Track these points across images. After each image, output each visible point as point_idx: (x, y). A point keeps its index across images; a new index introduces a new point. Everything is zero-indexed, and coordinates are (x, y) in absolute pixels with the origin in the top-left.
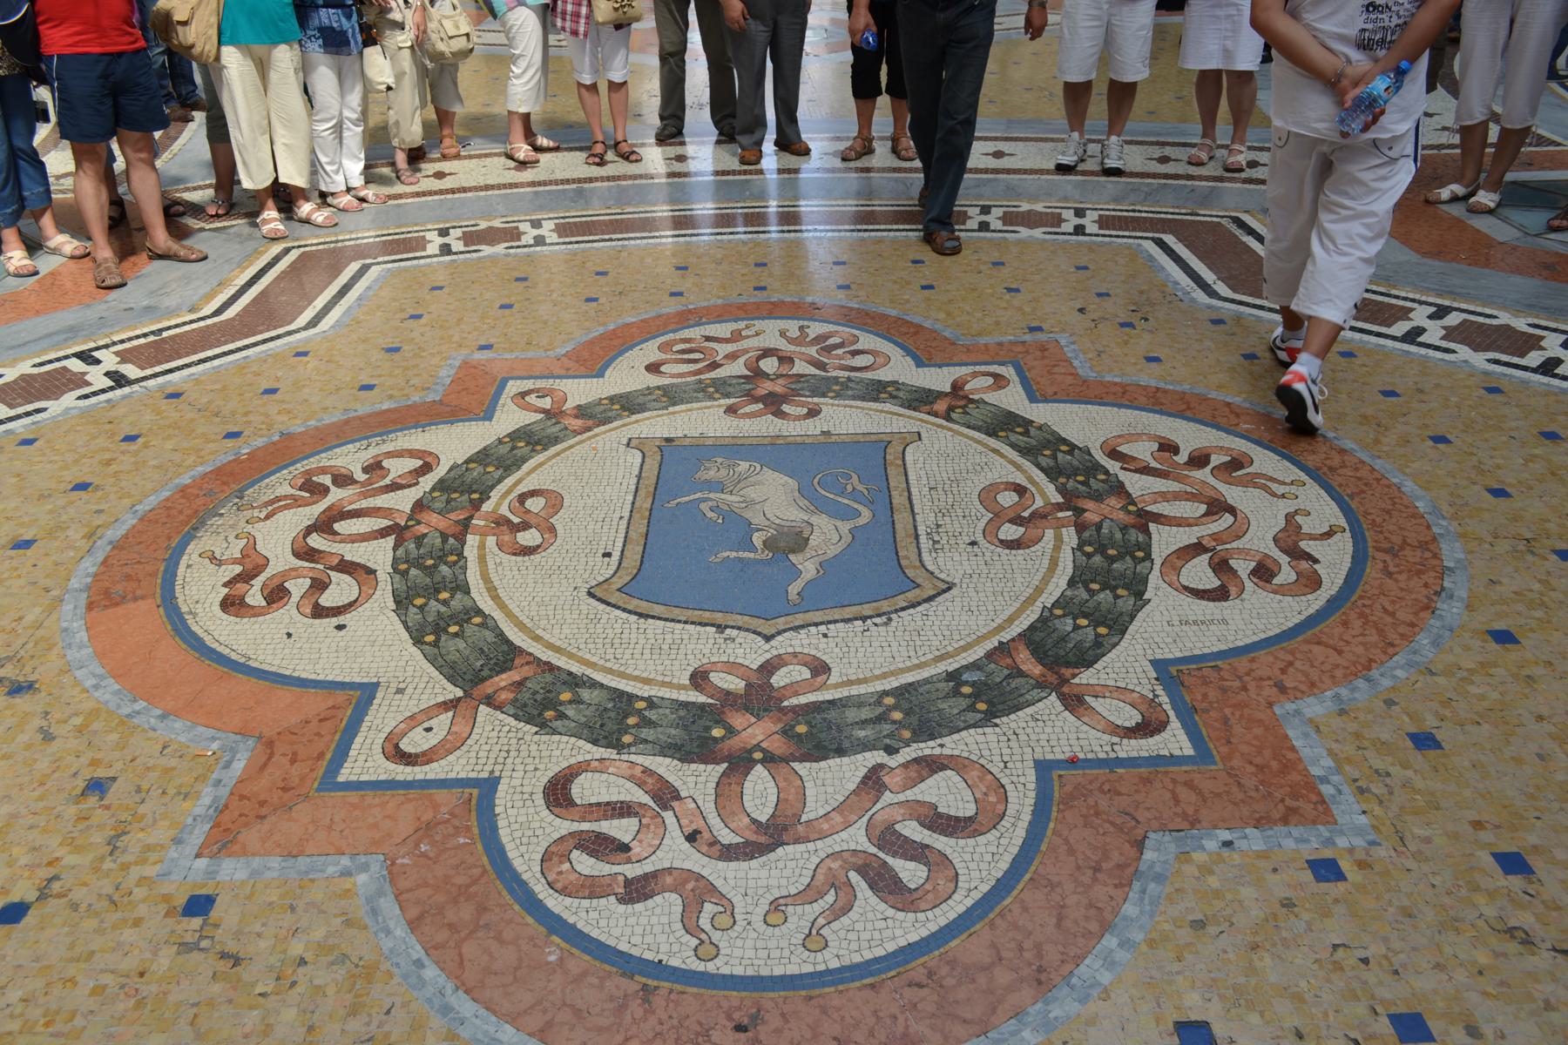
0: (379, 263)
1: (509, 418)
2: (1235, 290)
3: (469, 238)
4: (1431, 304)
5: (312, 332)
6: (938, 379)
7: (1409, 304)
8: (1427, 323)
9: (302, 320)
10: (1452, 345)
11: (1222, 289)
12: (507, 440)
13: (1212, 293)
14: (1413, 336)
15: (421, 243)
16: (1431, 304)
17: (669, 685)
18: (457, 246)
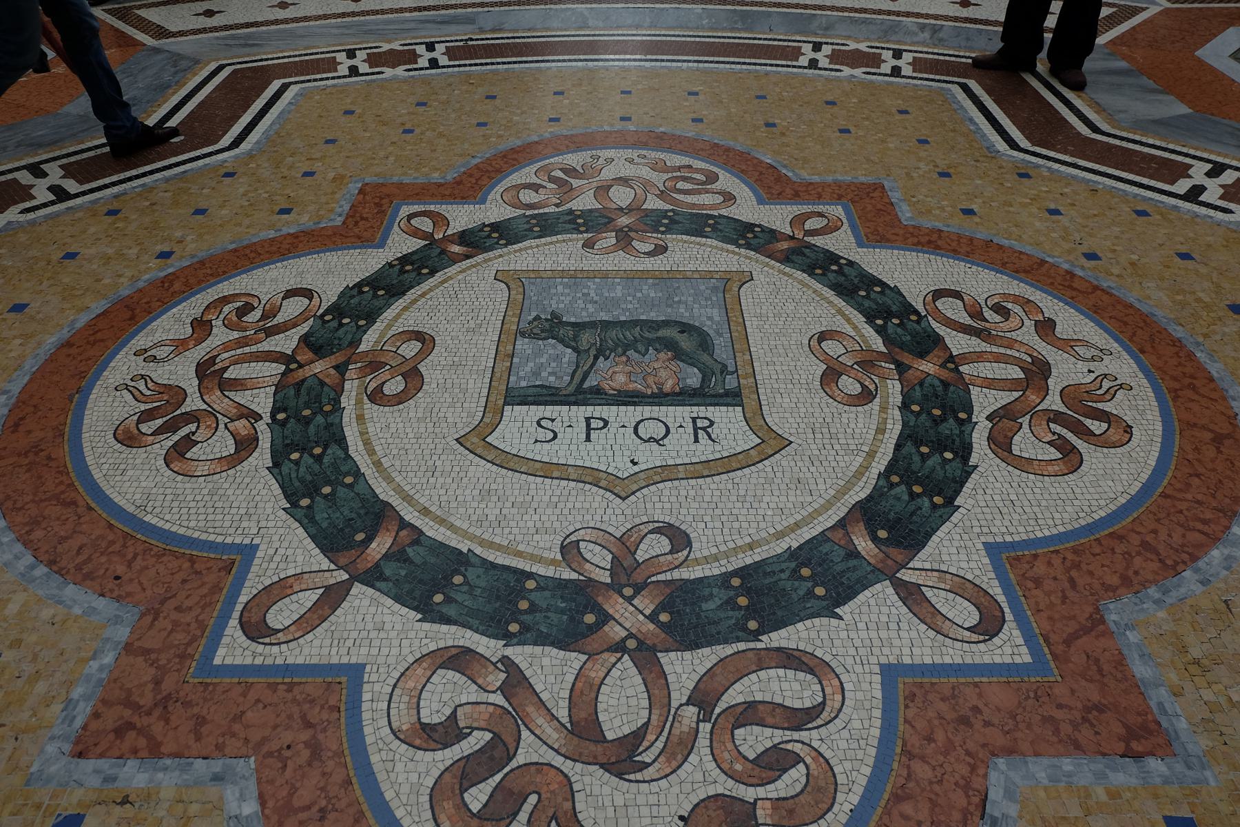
0: (296, 83)
1: (401, 244)
2: (1034, 144)
3: (374, 60)
4: (1208, 161)
5: (236, 151)
6: (778, 217)
7: (1188, 160)
8: (1207, 182)
9: (226, 140)
10: (1232, 206)
11: (1024, 143)
12: (396, 262)
13: (1013, 145)
14: (1194, 194)
15: (332, 65)
16: (1208, 161)
17: (540, 560)
18: (364, 68)
